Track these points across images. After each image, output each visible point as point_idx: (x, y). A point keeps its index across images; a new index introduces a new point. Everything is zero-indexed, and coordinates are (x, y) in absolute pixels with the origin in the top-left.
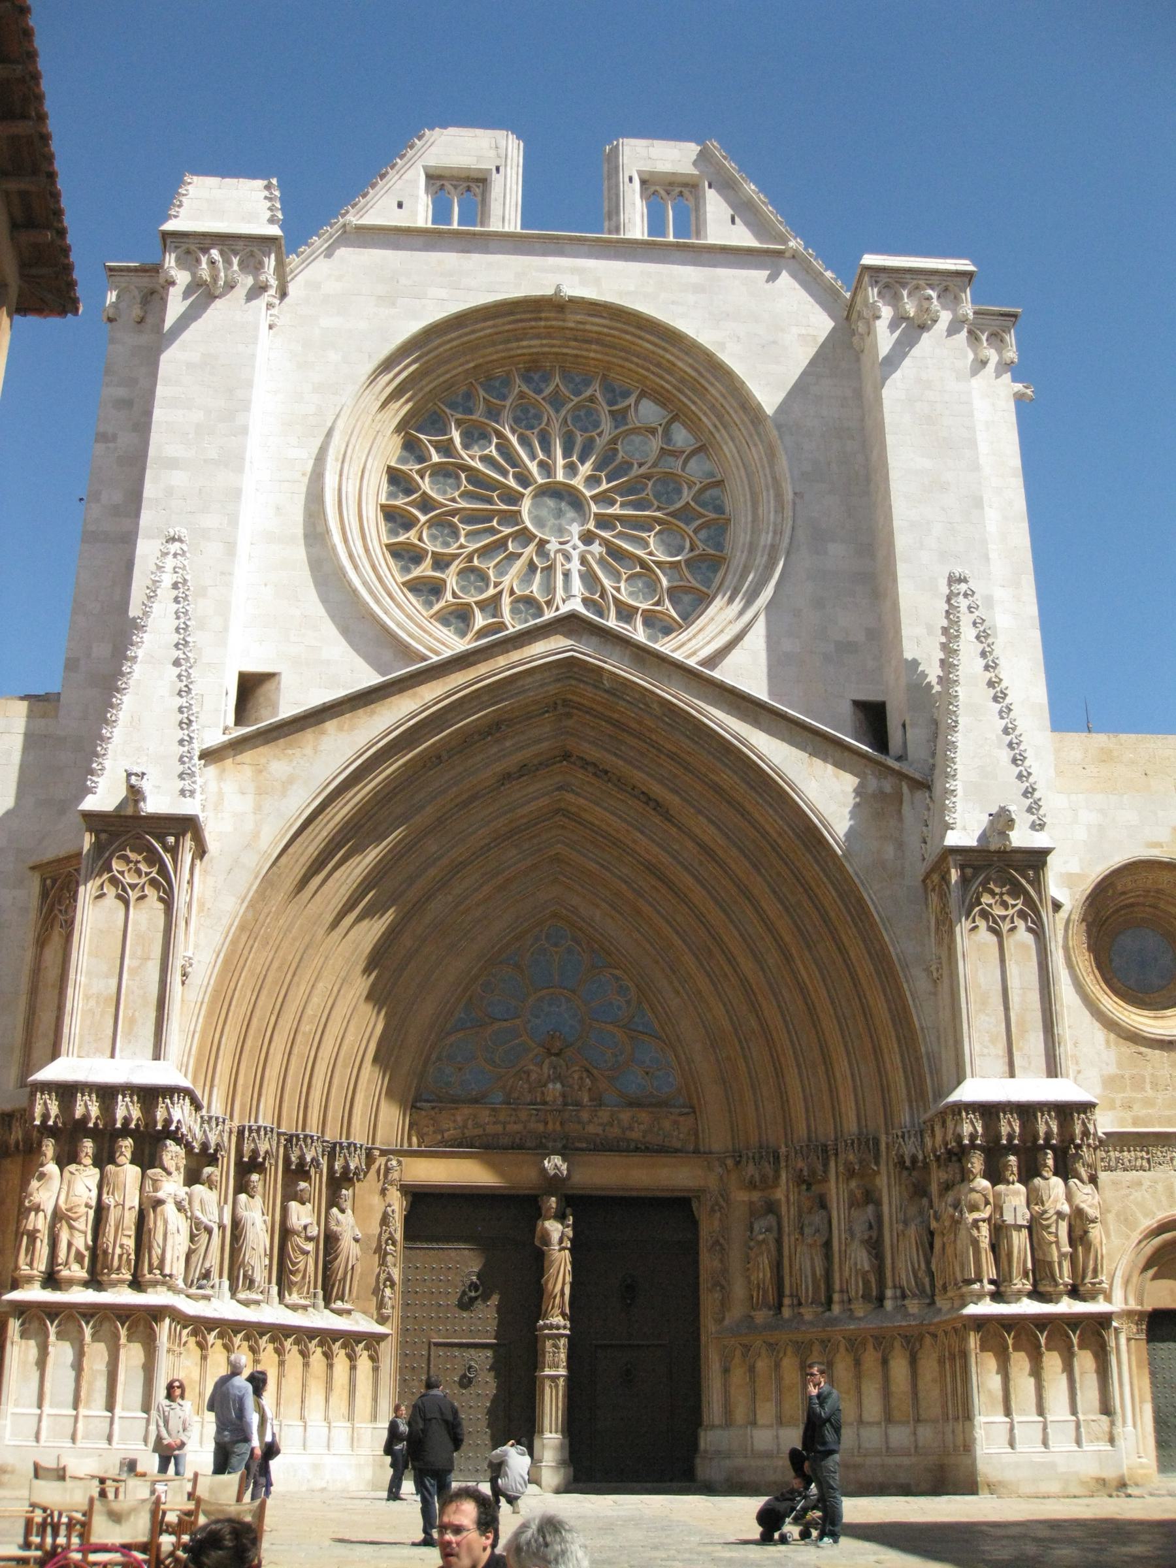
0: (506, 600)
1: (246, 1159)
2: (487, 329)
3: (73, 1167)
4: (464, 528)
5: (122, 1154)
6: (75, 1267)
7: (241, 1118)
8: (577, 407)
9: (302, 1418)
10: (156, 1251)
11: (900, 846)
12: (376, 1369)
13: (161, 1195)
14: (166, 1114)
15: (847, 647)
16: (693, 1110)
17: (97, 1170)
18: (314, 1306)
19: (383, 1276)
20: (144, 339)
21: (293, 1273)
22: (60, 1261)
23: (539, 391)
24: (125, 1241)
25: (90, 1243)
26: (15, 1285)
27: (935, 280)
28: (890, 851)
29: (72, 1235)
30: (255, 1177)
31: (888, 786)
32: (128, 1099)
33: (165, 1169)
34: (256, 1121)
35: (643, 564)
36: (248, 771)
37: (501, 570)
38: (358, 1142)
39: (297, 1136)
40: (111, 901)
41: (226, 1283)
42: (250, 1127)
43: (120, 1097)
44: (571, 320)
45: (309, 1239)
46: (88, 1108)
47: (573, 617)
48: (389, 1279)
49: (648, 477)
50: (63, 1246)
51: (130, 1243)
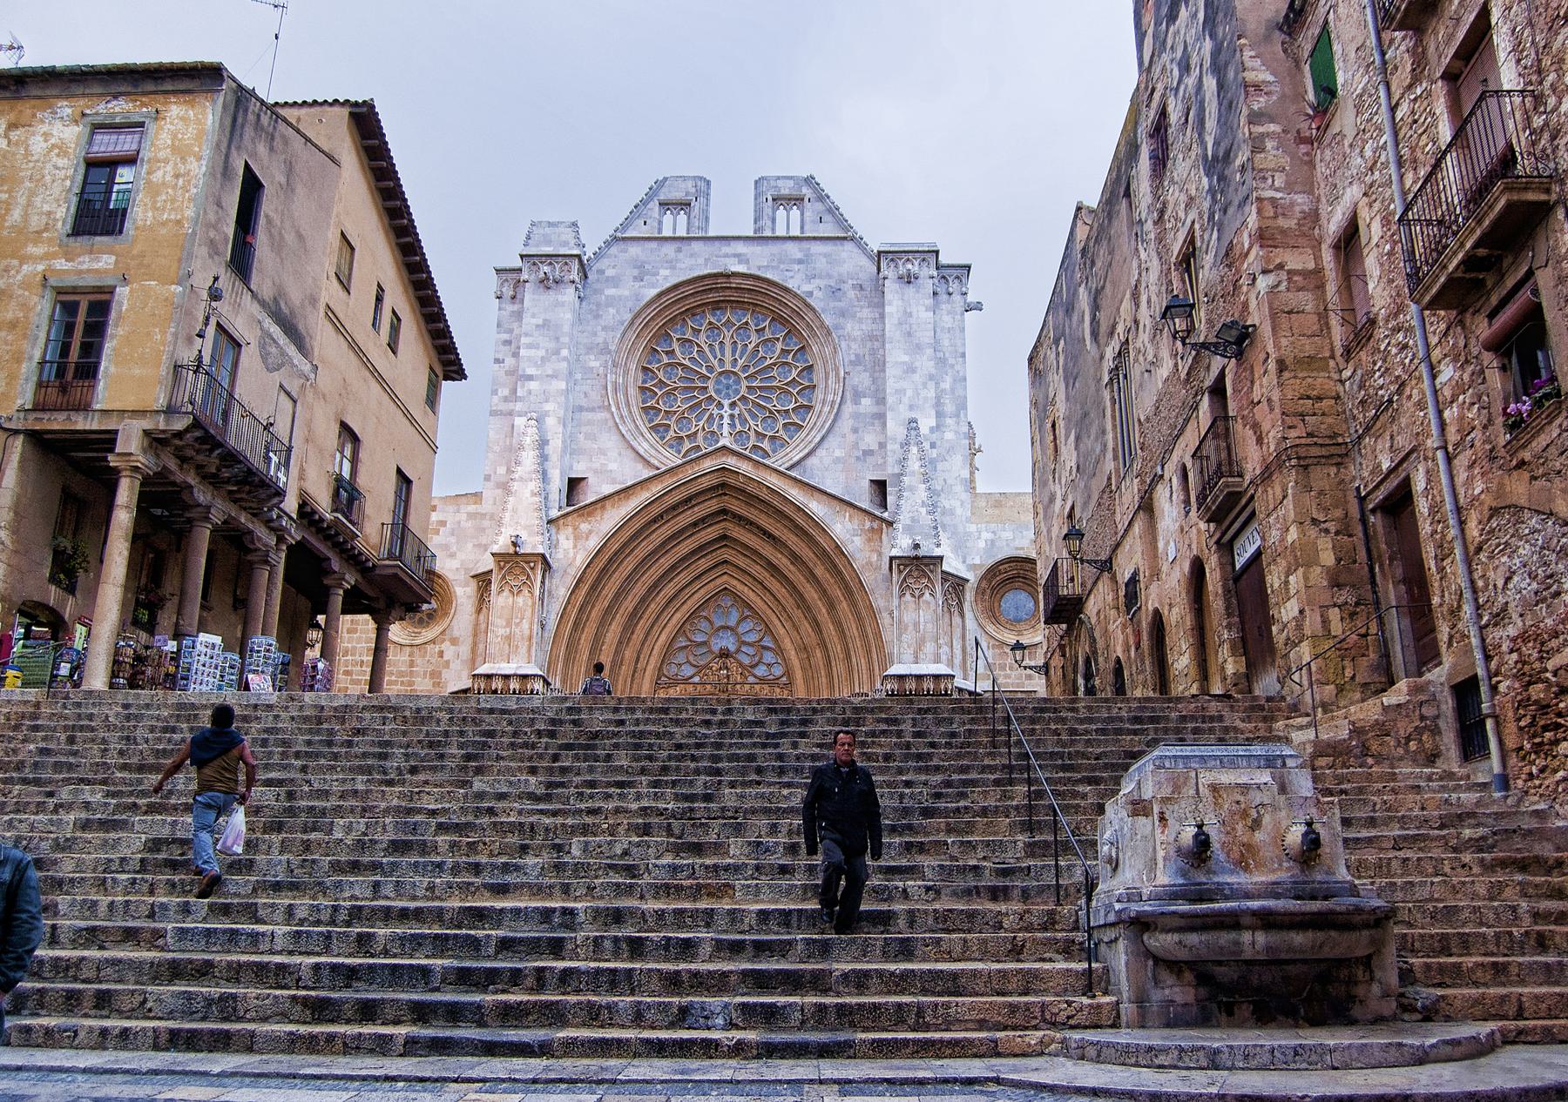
0: (700, 435)
2: (690, 290)
4: (680, 397)
8: (739, 328)
11: (880, 554)
15: (868, 453)
16: (790, 684)
20: (516, 307)
23: (719, 321)
27: (917, 255)
28: (875, 557)
31: (875, 525)
35: (771, 412)
36: (570, 529)
37: (698, 419)
40: (506, 593)
44: (735, 282)
46: (497, 684)
47: (724, 447)
49: (775, 364)
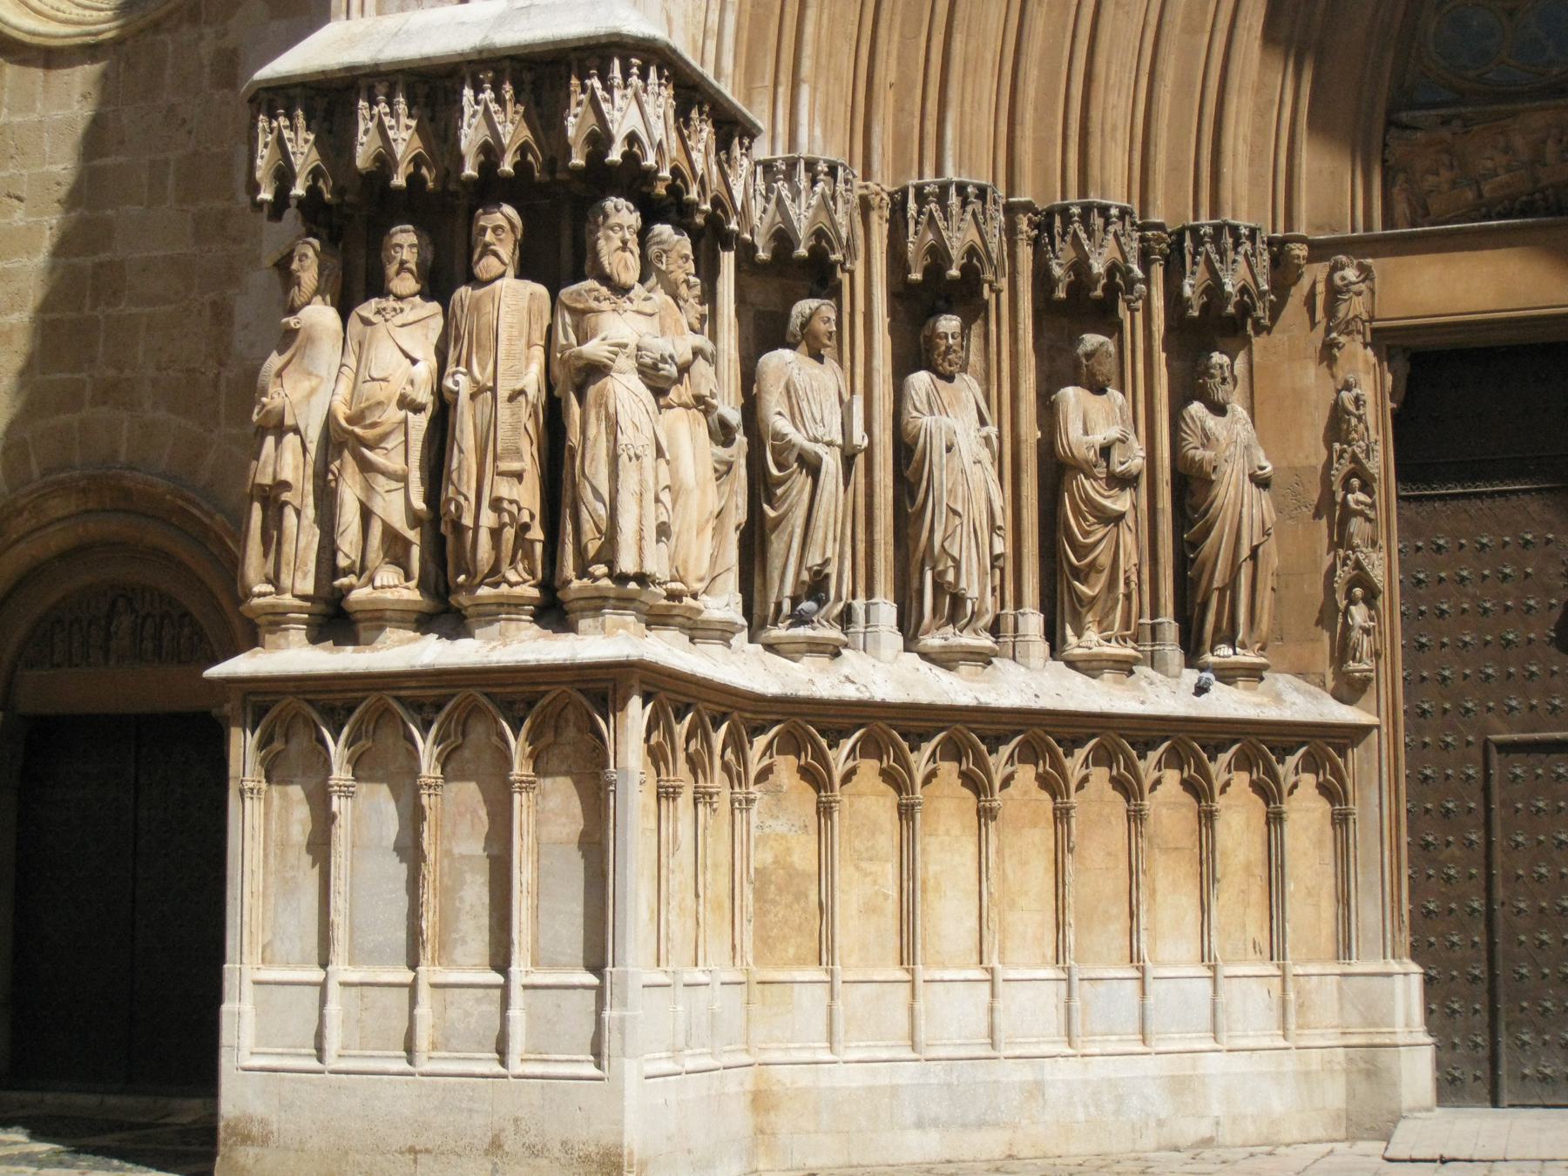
1: (916, 276)
3: (368, 309)
5: (487, 250)
6: (388, 575)
7: (900, 169)
9: (1134, 957)
10: (593, 511)
12: (1341, 820)
13: (594, 349)
14: (591, 120)
17: (434, 307)
18: (1153, 661)
19: (1343, 574)
21: (1078, 574)
22: (342, 562)
24: (505, 489)
25: (419, 504)
26: (250, 636)
29: (369, 488)
30: (949, 324)
32: (488, 95)
33: (606, 279)
34: (939, 171)
38: (1244, 223)
39: (1064, 211)
41: (886, 611)
42: (919, 189)
43: (468, 93)
45: (1124, 481)
48: (1361, 578)
50: (349, 516)
51: (527, 496)
